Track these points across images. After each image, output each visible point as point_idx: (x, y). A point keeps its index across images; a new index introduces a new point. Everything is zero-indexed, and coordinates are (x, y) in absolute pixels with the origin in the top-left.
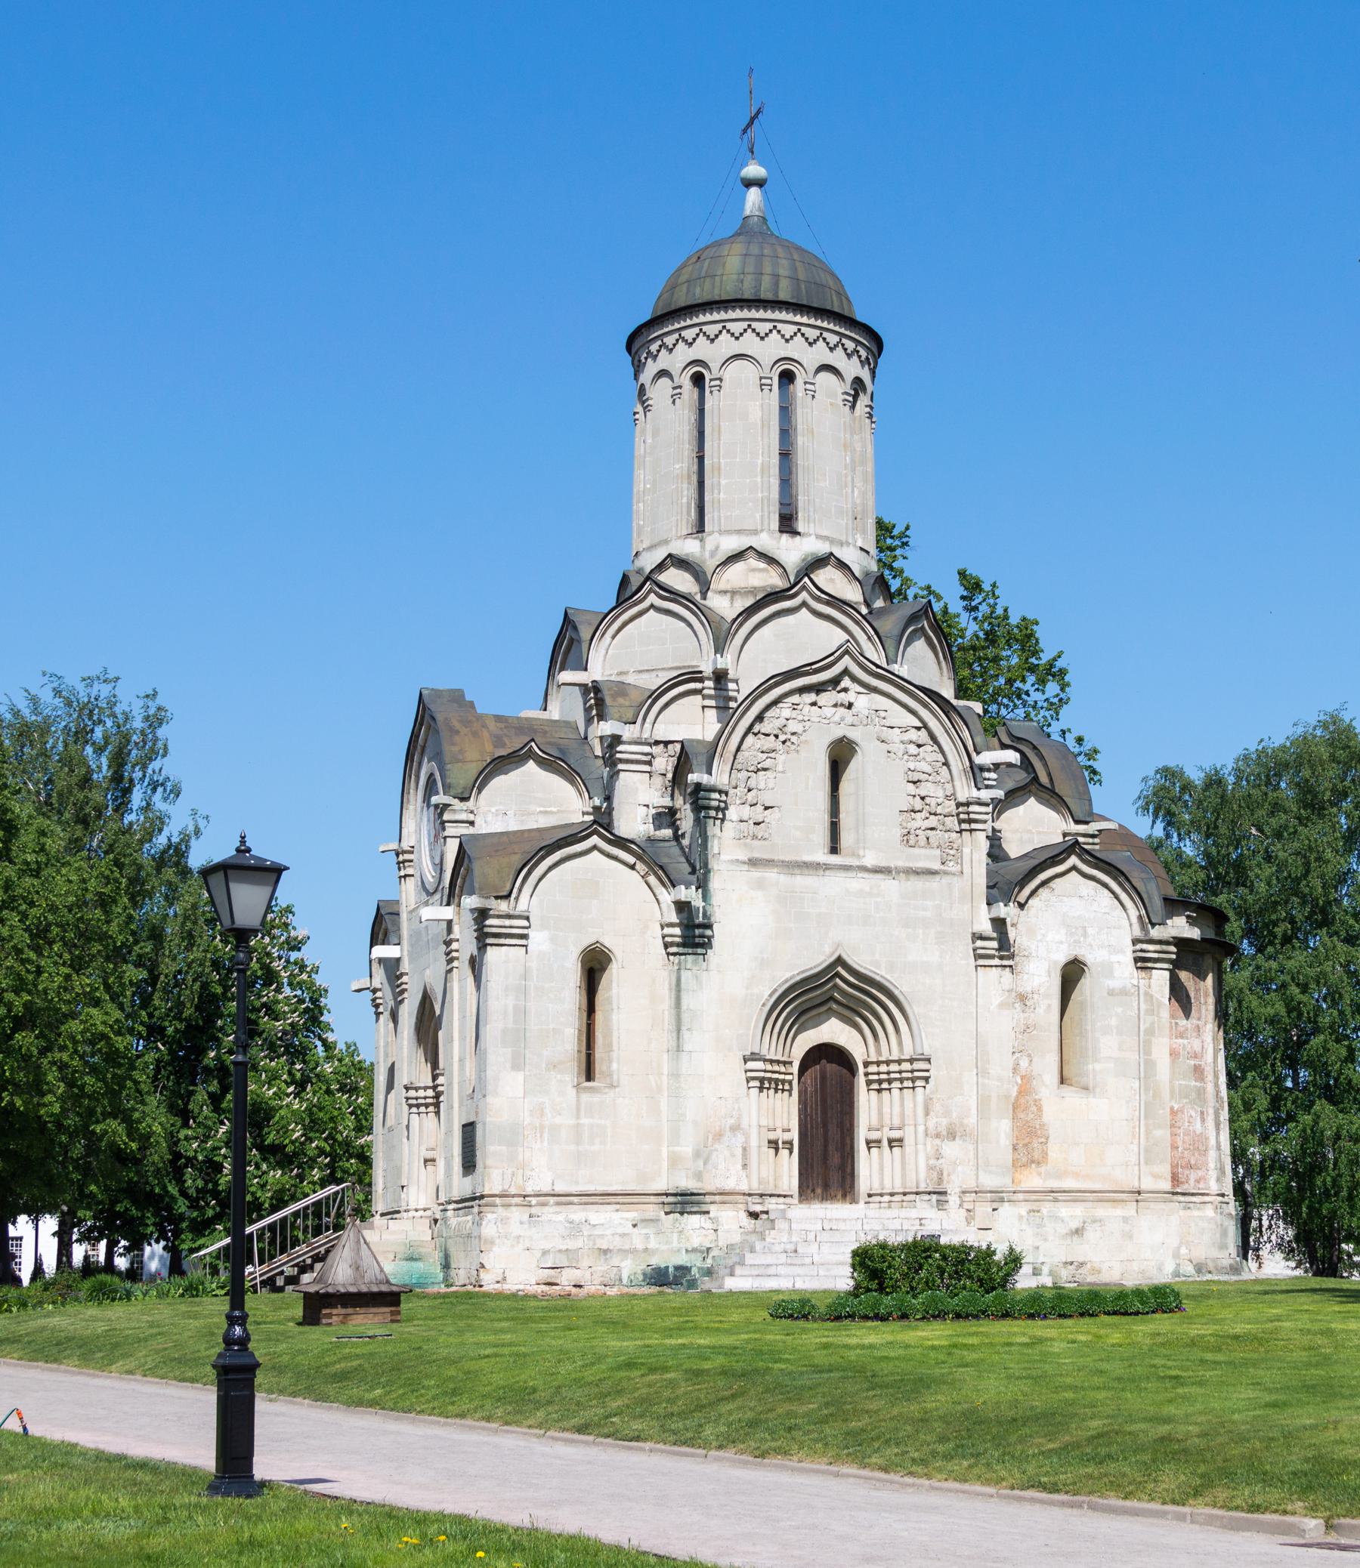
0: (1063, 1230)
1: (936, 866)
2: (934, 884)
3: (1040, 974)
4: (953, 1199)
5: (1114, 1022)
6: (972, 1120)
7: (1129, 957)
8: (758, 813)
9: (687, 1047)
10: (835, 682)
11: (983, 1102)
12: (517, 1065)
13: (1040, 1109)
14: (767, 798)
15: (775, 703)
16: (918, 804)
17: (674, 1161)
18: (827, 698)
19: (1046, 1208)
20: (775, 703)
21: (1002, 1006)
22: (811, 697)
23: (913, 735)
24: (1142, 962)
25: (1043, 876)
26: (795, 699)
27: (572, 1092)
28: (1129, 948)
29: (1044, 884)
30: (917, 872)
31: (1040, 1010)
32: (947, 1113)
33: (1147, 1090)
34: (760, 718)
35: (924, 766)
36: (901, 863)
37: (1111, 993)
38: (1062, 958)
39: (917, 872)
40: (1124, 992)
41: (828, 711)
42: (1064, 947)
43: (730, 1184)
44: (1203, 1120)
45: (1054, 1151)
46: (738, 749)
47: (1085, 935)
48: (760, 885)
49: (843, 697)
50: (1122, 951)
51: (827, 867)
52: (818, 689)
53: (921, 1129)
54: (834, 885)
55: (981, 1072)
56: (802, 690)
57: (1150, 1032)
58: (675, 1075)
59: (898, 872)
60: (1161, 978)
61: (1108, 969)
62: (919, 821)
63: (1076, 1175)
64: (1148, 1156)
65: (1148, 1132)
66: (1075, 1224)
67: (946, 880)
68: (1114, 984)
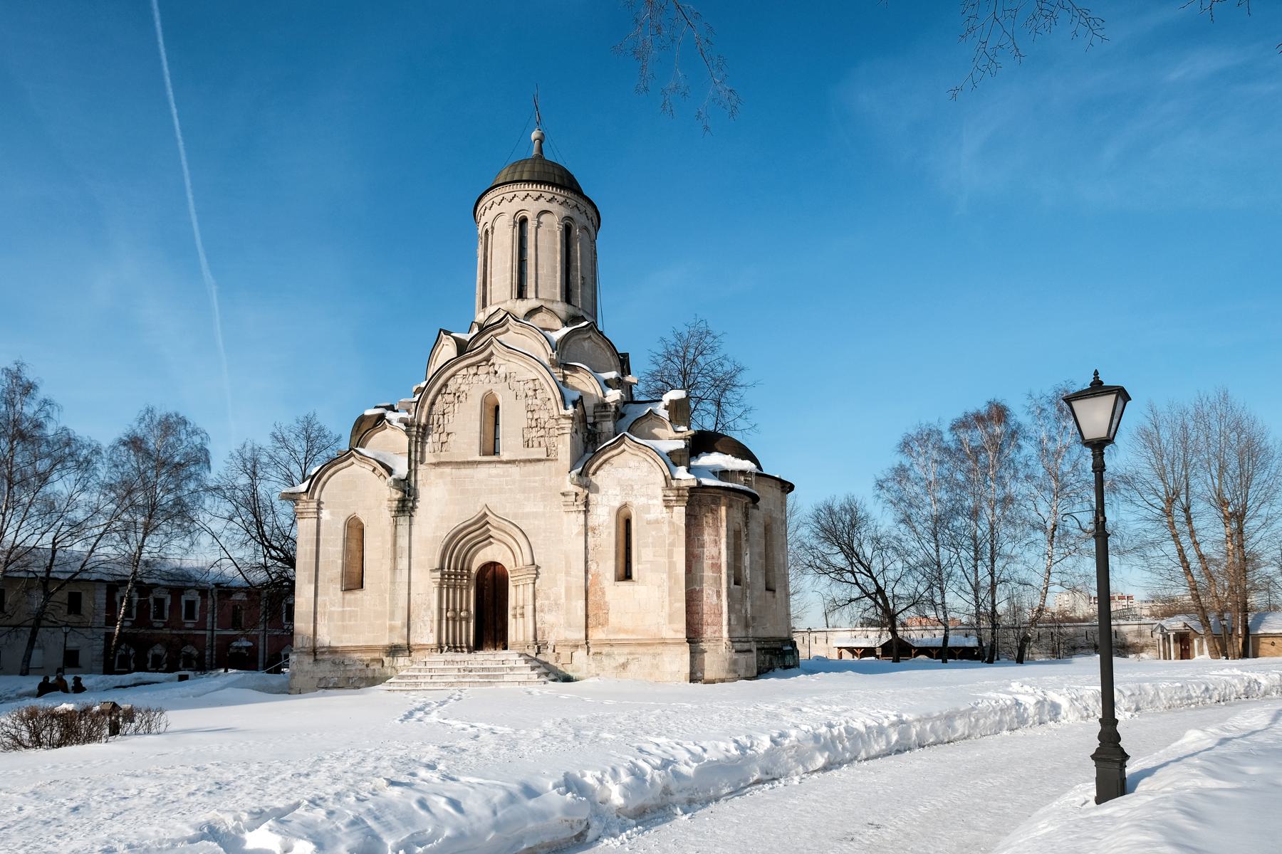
0: (614, 664)
1: (544, 457)
2: (540, 466)
3: (603, 515)
4: (551, 648)
5: (650, 540)
6: (563, 601)
7: (661, 498)
8: (444, 437)
9: (400, 567)
10: (487, 360)
11: (568, 590)
12: (309, 582)
13: (604, 593)
14: (448, 429)
15: (453, 375)
16: (534, 424)
17: (392, 629)
18: (483, 370)
19: (605, 650)
20: (453, 375)
21: (578, 534)
22: (473, 370)
23: (531, 385)
24: (668, 504)
25: (605, 457)
26: (464, 372)
27: (340, 593)
28: (660, 493)
29: (605, 461)
30: (530, 461)
31: (604, 536)
32: (548, 598)
33: (670, 578)
34: (445, 385)
35: (538, 402)
36: (523, 457)
37: (649, 523)
38: (617, 504)
39: (530, 461)
40: (657, 522)
41: (483, 377)
42: (619, 498)
43: (424, 641)
44: (719, 595)
45: (613, 619)
46: (433, 403)
47: (632, 489)
48: (441, 476)
49: (491, 369)
50: (656, 497)
51: (480, 463)
52: (477, 364)
53: (531, 607)
54: (483, 471)
55: (568, 573)
56: (467, 367)
57: (672, 545)
58: (393, 582)
59: (520, 461)
60: (680, 512)
61: (647, 509)
62: (534, 433)
63: (626, 632)
64: (671, 619)
65: (671, 604)
66: (622, 660)
67: (548, 464)
68: (651, 516)
